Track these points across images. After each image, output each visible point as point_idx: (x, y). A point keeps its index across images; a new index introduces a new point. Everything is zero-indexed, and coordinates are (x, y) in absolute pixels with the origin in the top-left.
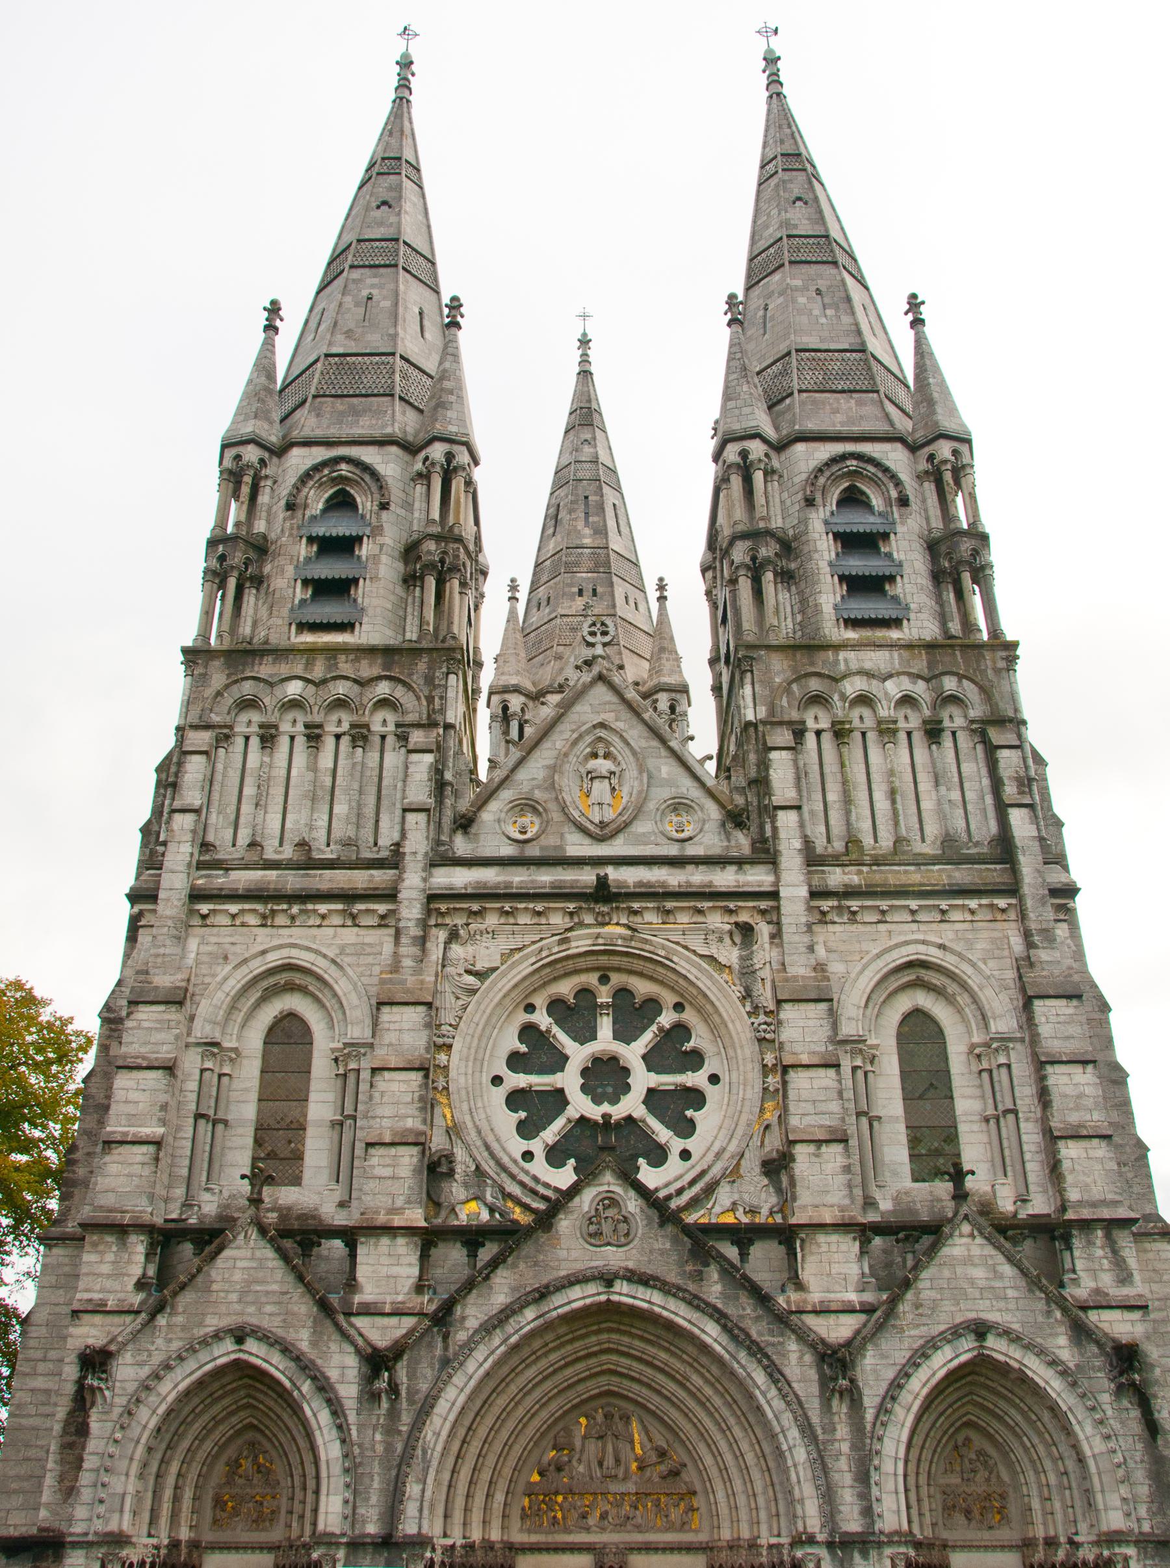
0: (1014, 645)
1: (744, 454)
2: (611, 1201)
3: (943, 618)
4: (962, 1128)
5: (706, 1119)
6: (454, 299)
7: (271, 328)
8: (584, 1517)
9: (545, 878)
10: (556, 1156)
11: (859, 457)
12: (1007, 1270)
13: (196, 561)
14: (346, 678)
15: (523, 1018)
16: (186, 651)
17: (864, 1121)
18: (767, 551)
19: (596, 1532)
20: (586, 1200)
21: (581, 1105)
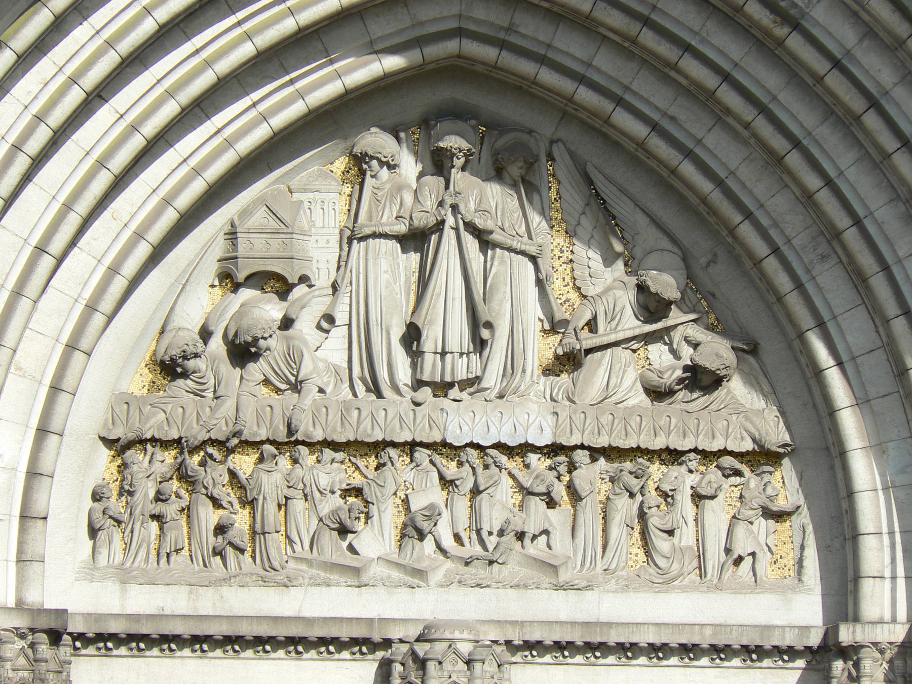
8: (343, 531)
19: (385, 583)
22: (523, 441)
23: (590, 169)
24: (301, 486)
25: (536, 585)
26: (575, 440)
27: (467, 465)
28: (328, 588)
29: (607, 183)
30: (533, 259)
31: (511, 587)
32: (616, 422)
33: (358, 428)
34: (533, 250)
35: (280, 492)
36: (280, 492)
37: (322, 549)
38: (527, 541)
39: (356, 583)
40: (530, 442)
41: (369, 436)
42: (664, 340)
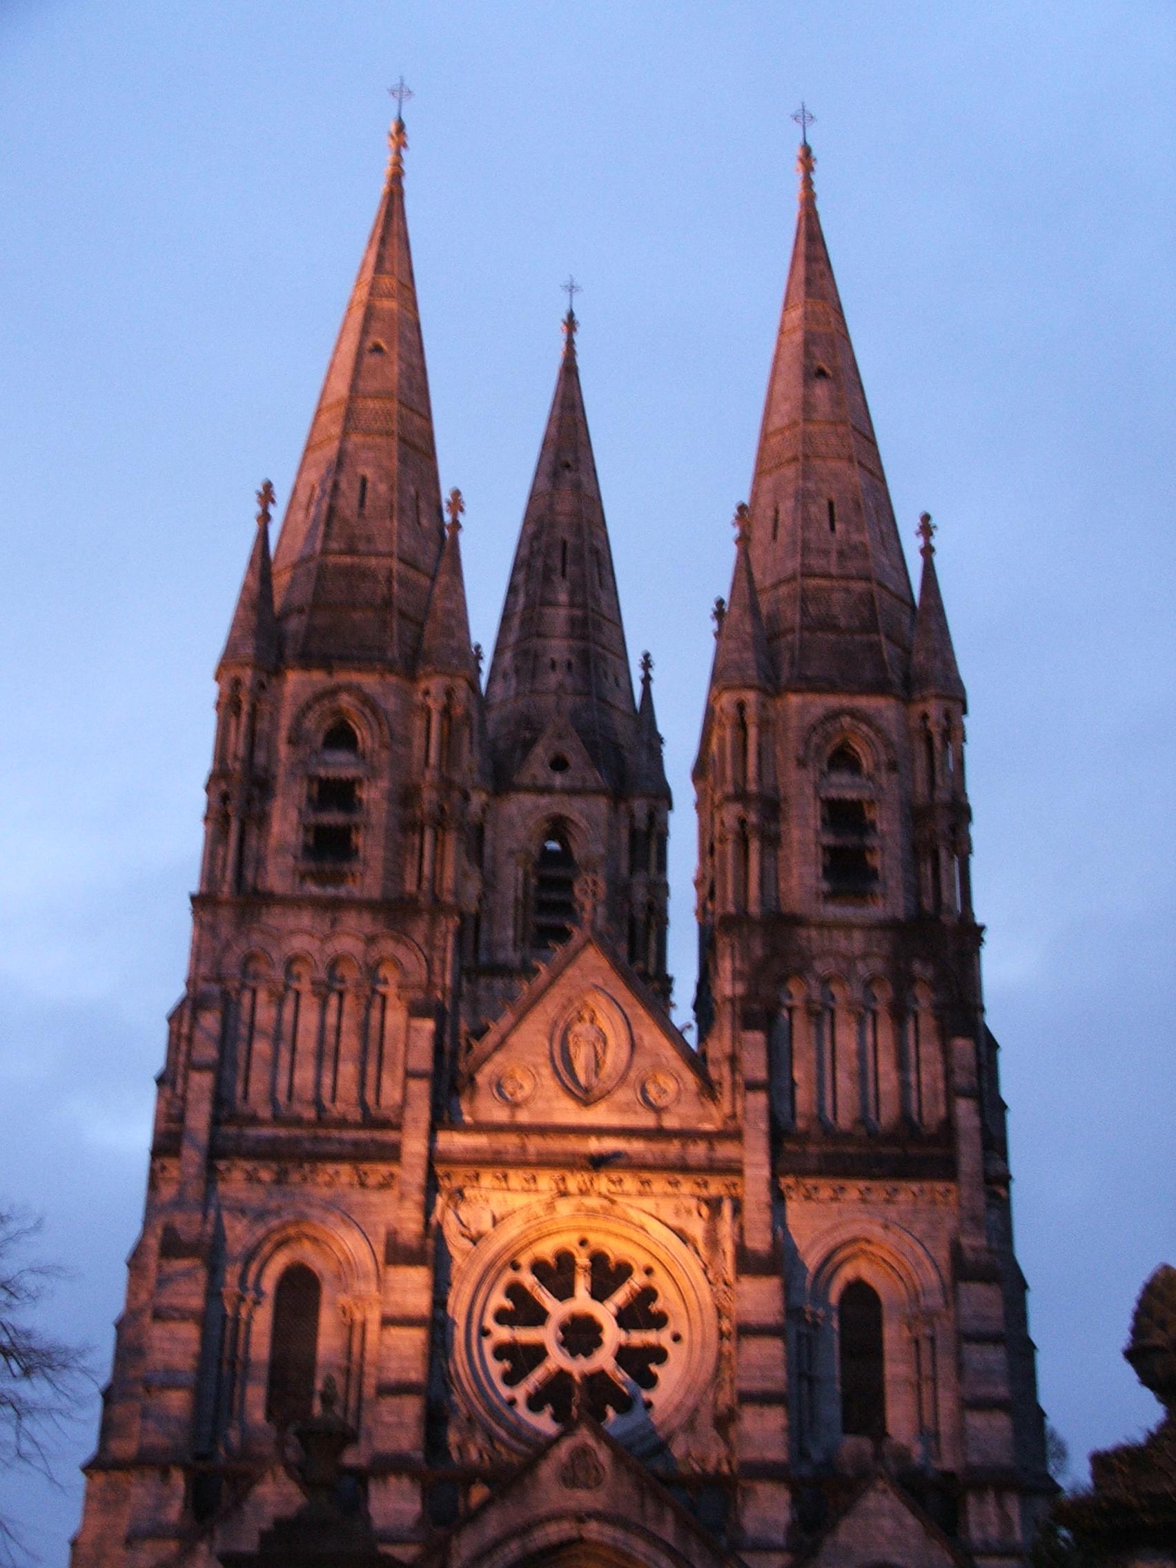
0: (982, 928)
1: (741, 706)
2: (582, 1452)
3: (915, 891)
4: (889, 1389)
5: (670, 1376)
6: (456, 494)
7: (265, 518)
9: (535, 1144)
10: (535, 1403)
11: (854, 714)
12: (911, 1521)
13: (198, 801)
14: (348, 934)
15: (509, 1275)
16: (194, 899)
17: (805, 1384)
18: (753, 818)
20: (563, 1451)
21: (557, 1359)
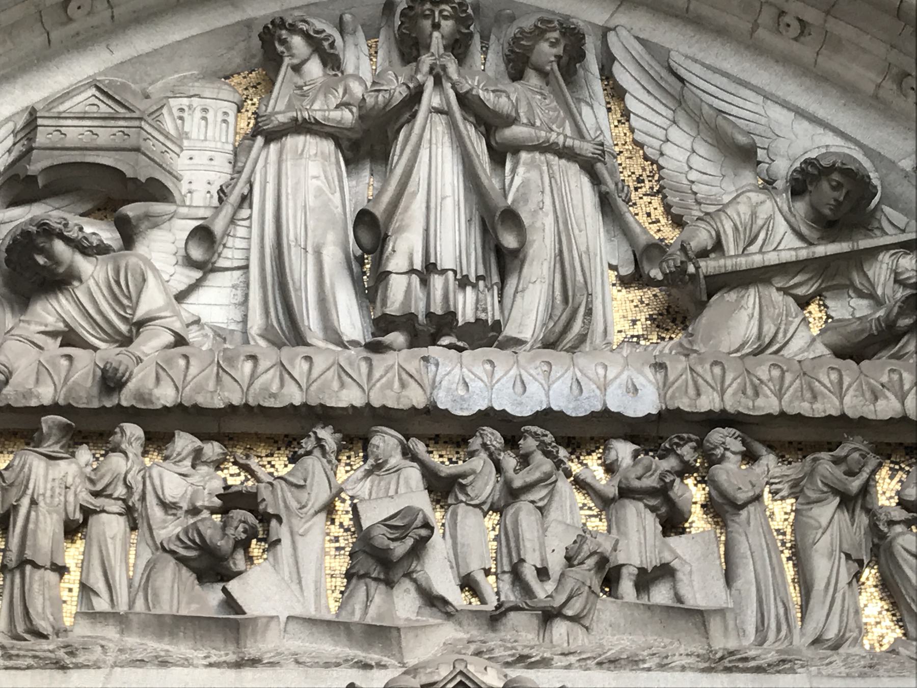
22: (598, 407)
23: (676, 59)
24: (120, 491)
25: (656, 660)
26: (708, 402)
27: (484, 455)
28: (163, 671)
29: (709, 75)
30: (589, 167)
31: (600, 664)
32: (788, 377)
33: (250, 385)
34: (587, 149)
35: (71, 498)
36: (71, 498)
37: (156, 595)
38: (627, 587)
39: (232, 658)
40: (613, 409)
41: (274, 396)
42: (852, 285)
